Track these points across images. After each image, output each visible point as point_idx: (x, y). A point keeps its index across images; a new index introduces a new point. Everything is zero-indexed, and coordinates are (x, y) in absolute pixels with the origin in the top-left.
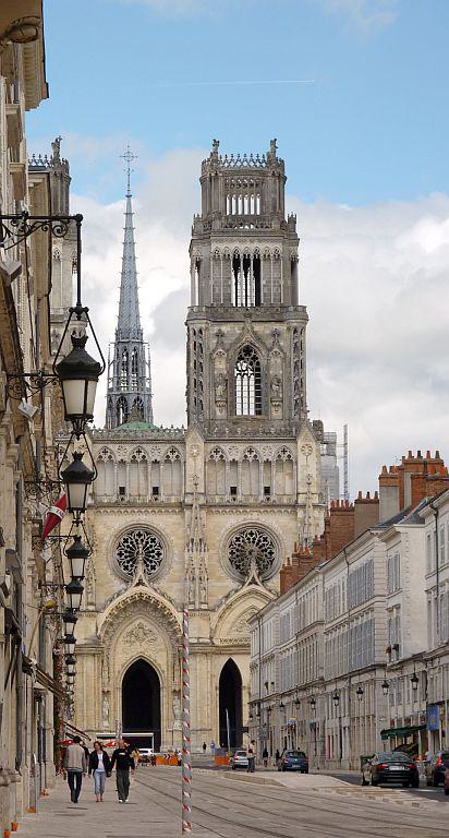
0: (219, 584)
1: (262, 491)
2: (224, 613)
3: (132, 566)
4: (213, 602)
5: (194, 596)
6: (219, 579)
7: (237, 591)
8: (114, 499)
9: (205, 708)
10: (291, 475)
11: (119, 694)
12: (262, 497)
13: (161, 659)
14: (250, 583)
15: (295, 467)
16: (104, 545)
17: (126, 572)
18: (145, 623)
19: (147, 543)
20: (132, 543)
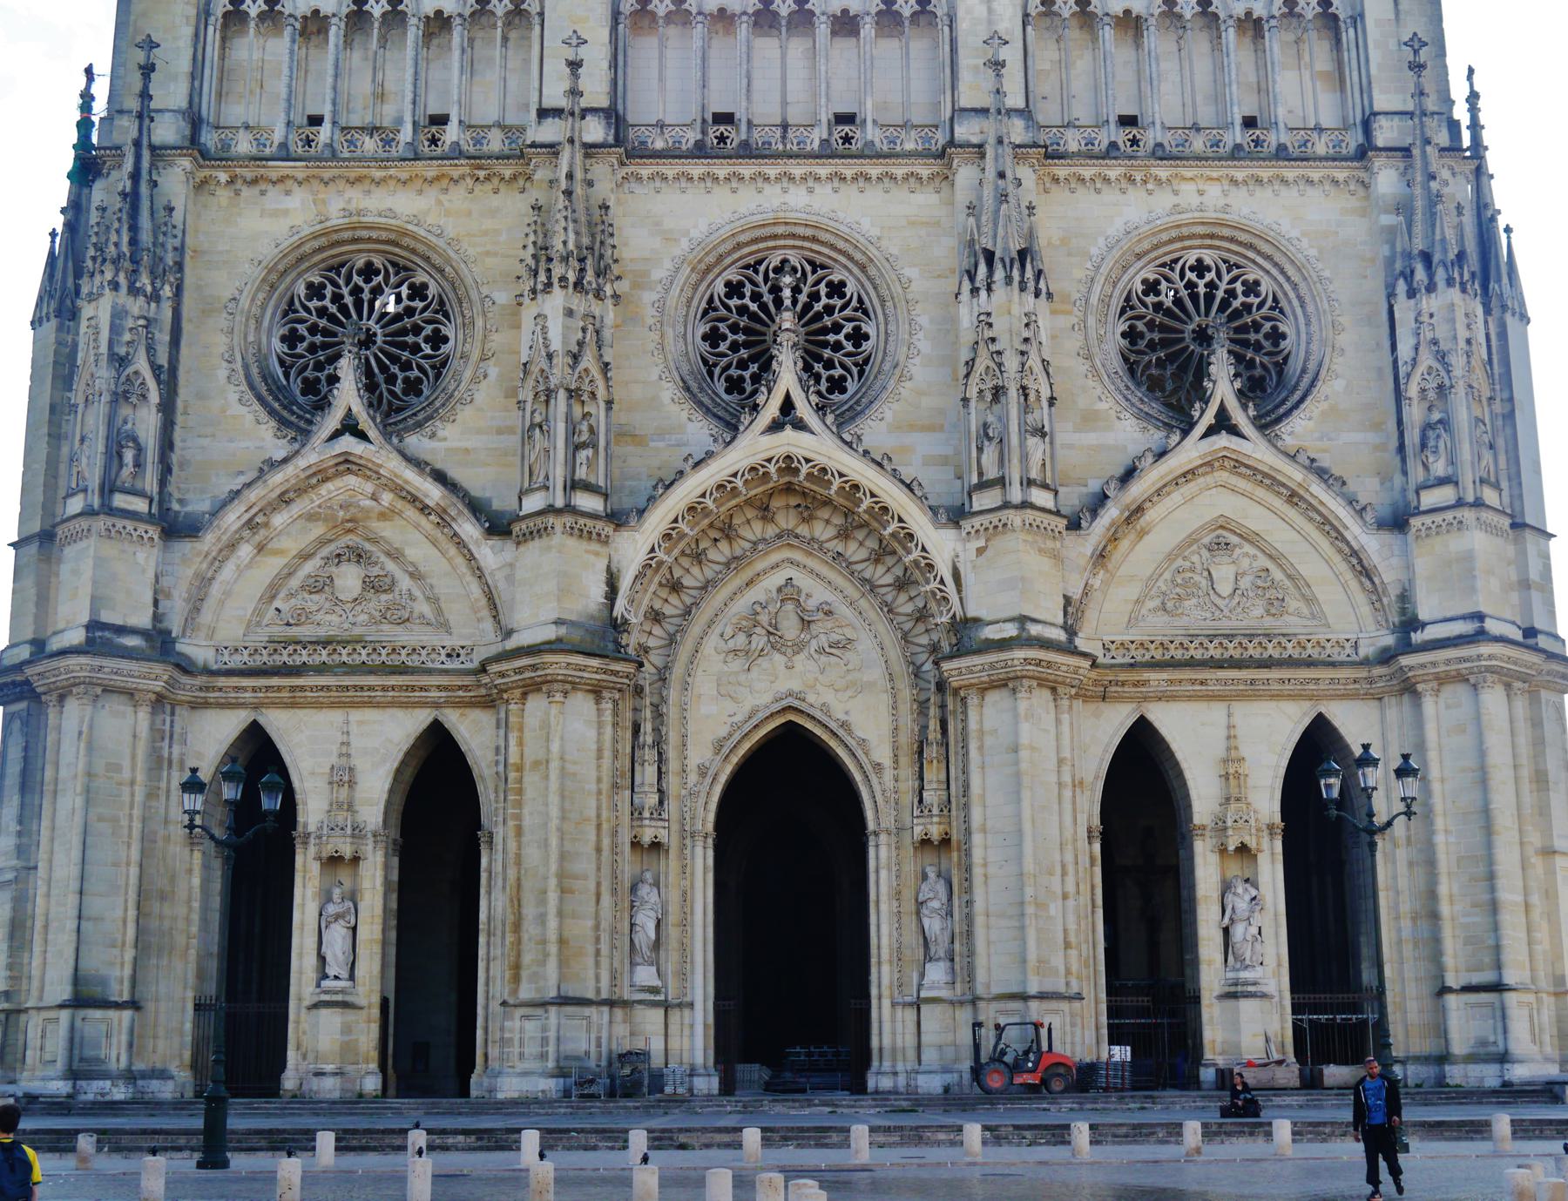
0: (1091, 438)
1: (1238, 121)
2: (1114, 539)
3: (756, 379)
4: (1071, 498)
5: (1001, 461)
6: (1089, 419)
7: (1161, 454)
8: (692, 136)
9: (1054, 909)
10: (1339, 78)
11: (703, 859)
12: (1237, 135)
13: (865, 720)
14: (1211, 431)
15: (1348, 36)
16: (649, 297)
17: (733, 398)
18: (803, 581)
19: (815, 297)
20: (756, 297)
